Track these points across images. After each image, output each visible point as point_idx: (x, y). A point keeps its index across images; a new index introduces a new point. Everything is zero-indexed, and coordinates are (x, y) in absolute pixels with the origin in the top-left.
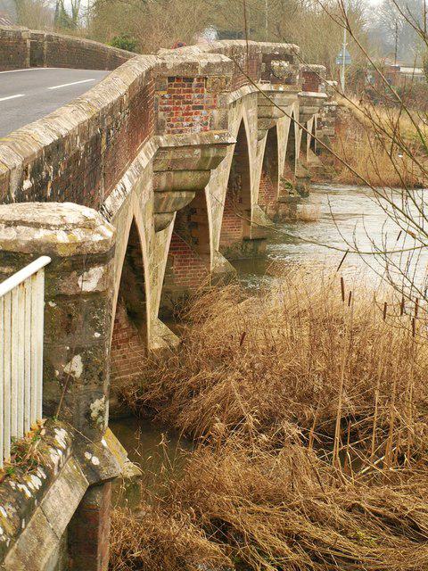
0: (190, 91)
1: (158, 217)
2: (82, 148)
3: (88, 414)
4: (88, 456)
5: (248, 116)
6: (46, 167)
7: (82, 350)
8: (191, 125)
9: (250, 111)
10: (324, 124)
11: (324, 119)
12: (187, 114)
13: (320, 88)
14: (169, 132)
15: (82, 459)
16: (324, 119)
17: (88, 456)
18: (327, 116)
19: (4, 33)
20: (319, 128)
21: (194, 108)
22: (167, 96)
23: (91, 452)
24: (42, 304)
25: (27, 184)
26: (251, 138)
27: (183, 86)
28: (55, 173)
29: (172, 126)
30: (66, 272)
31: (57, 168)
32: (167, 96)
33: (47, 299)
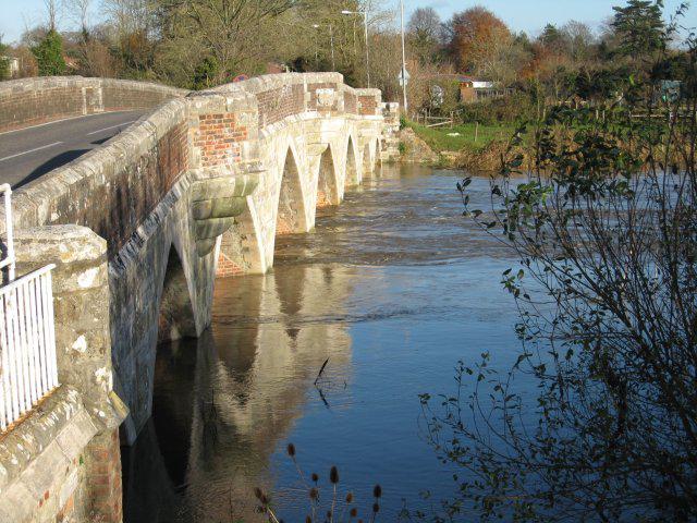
0: (222, 127)
1: (200, 243)
2: (108, 185)
3: (93, 379)
4: (96, 410)
5: (295, 144)
6: (71, 202)
7: (85, 331)
8: (224, 157)
9: (297, 139)
10: (388, 144)
11: (388, 140)
12: (221, 147)
13: (376, 110)
14: (204, 165)
15: (91, 413)
16: (388, 140)
17: (96, 410)
18: (391, 137)
19: (4, 98)
20: (384, 150)
21: (226, 141)
22: (199, 132)
23: (98, 407)
24: (51, 299)
25: (54, 217)
26: (301, 163)
27: (214, 122)
28: (82, 205)
29: (206, 159)
30: (68, 274)
31: (82, 201)
32: (199, 132)
33: (55, 295)
